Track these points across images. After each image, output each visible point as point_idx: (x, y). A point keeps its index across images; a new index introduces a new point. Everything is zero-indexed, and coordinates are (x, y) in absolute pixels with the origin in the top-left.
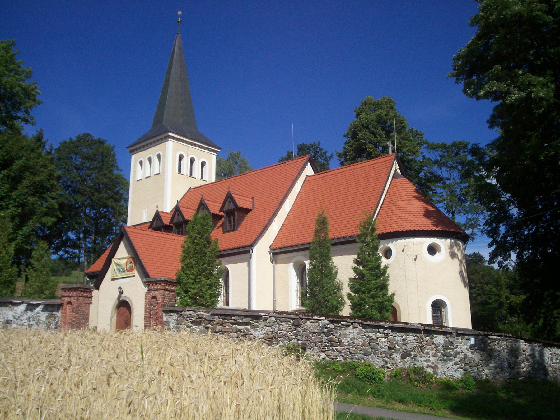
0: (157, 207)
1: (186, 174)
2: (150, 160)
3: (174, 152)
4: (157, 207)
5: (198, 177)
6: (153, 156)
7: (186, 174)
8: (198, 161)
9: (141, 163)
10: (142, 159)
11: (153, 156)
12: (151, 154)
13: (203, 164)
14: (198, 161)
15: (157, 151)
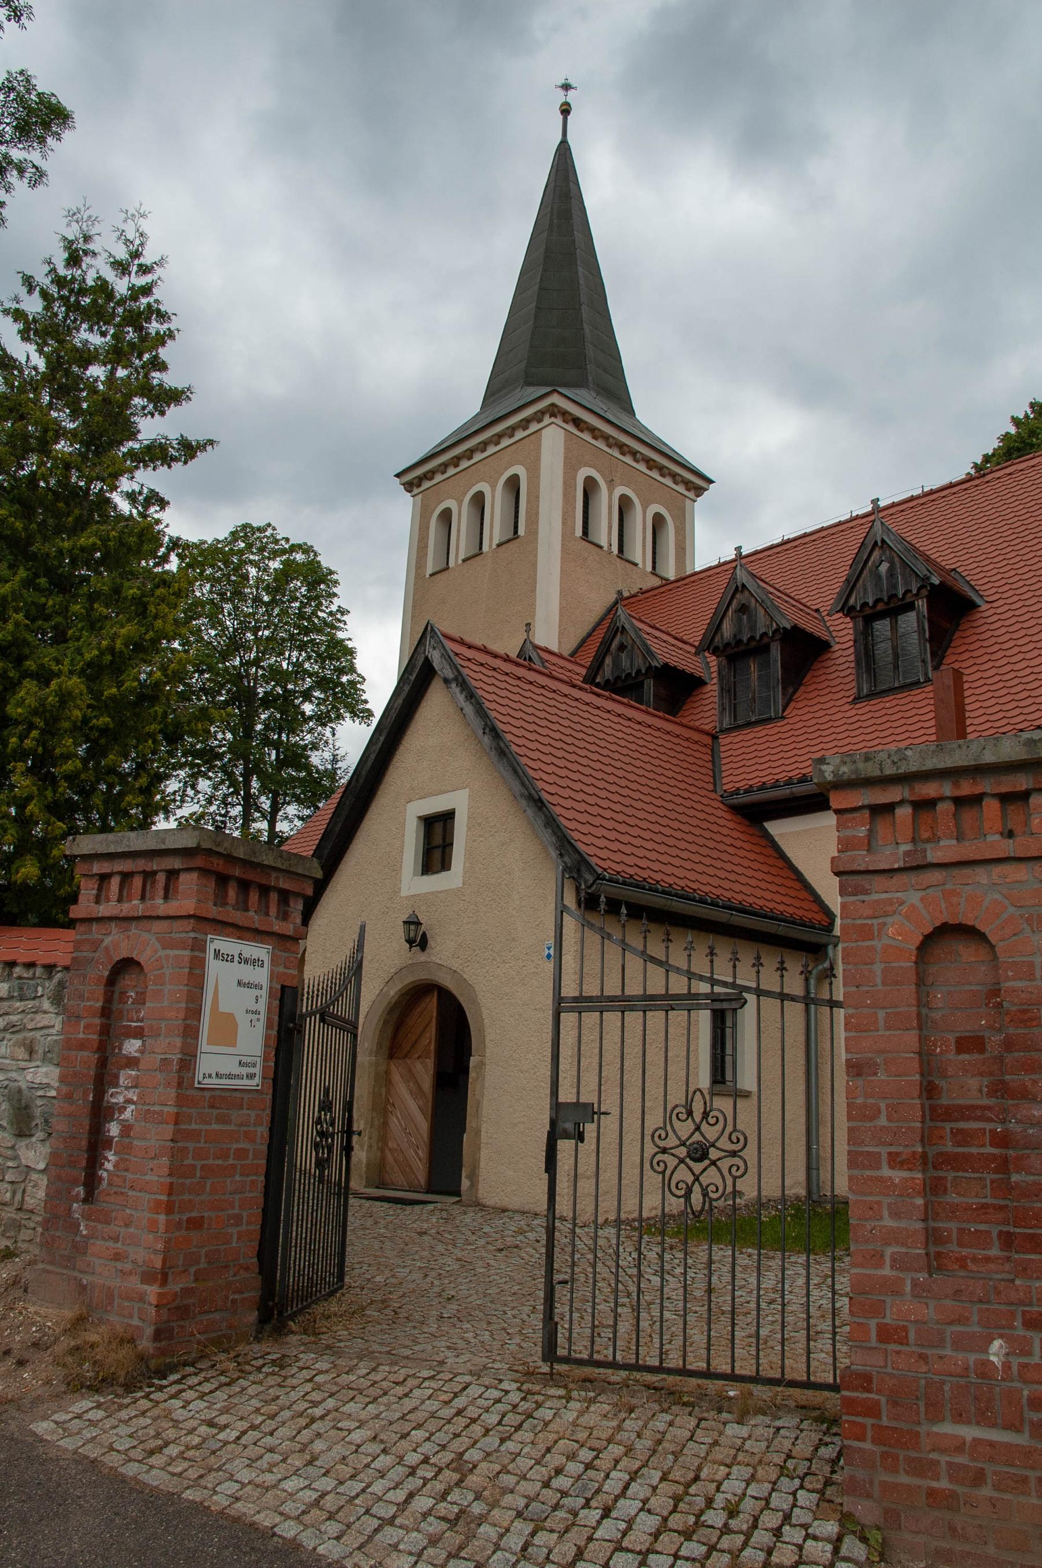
0: (528, 631)
1: (606, 548)
2: (479, 499)
3: (570, 467)
4: (528, 631)
5: (644, 562)
6: (493, 487)
7: (606, 548)
8: (644, 513)
9: (446, 516)
10: (451, 504)
11: (493, 487)
12: (482, 480)
13: (658, 522)
14: (644, 513)
15: (506, 469)
